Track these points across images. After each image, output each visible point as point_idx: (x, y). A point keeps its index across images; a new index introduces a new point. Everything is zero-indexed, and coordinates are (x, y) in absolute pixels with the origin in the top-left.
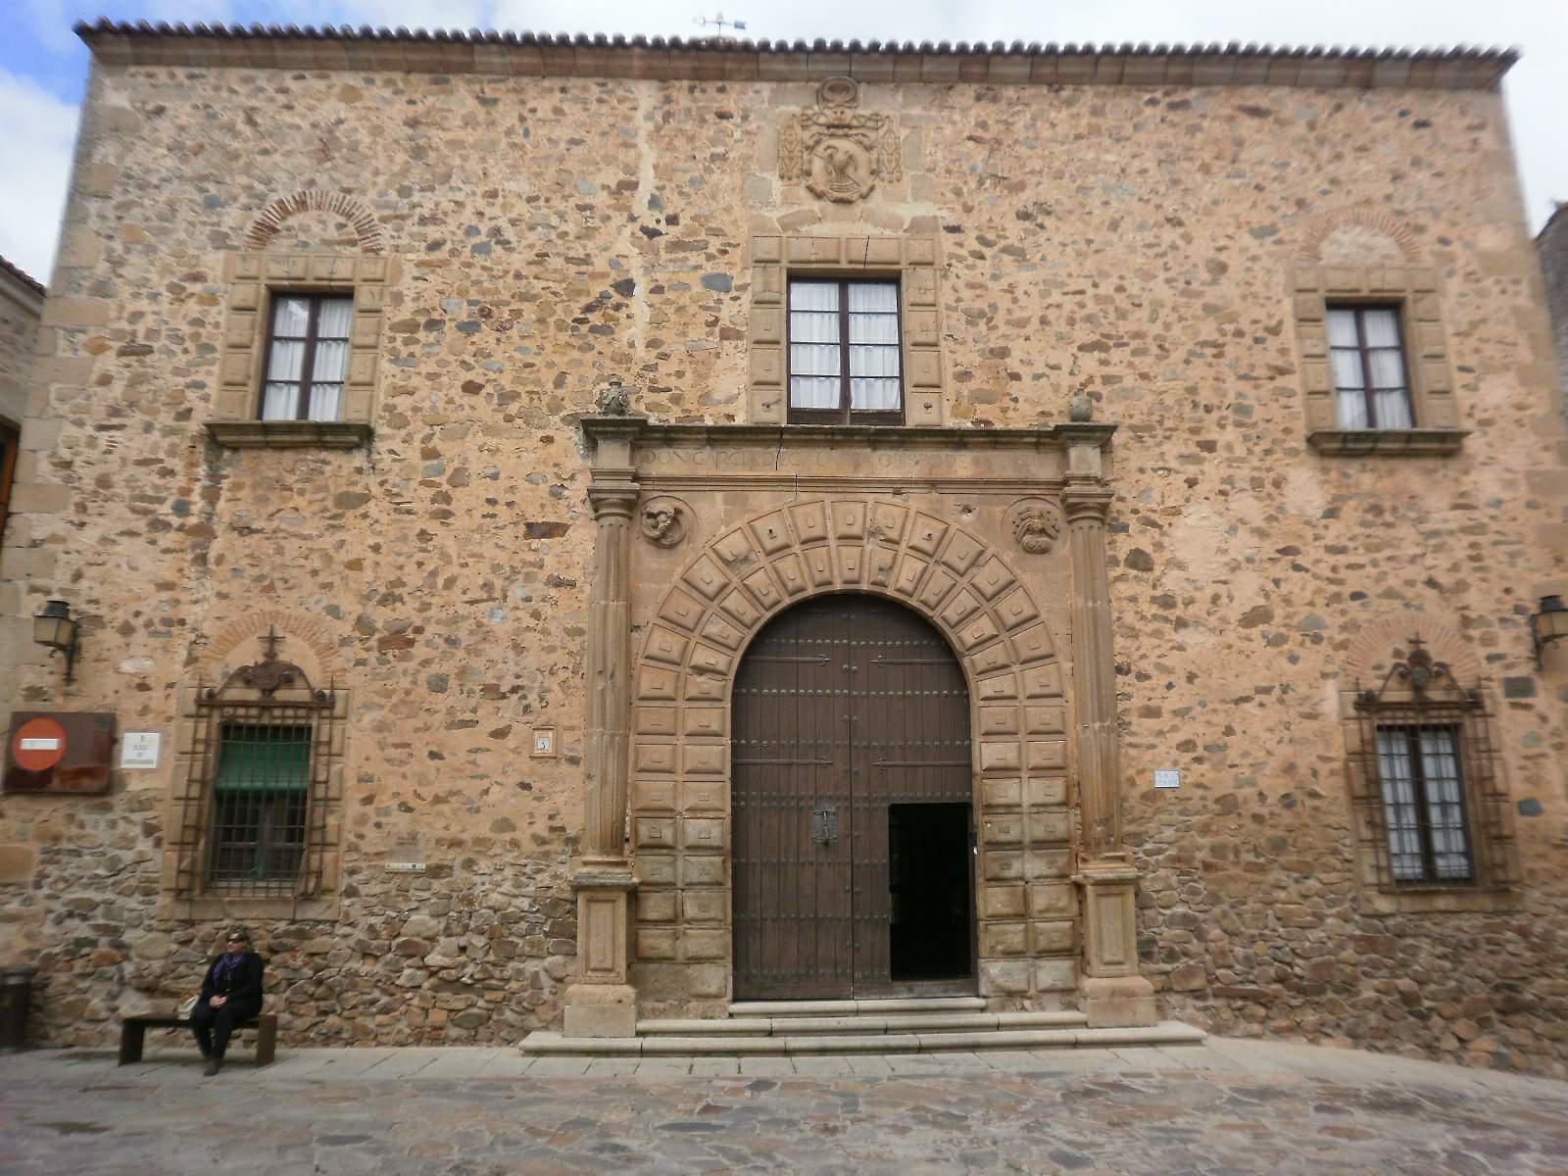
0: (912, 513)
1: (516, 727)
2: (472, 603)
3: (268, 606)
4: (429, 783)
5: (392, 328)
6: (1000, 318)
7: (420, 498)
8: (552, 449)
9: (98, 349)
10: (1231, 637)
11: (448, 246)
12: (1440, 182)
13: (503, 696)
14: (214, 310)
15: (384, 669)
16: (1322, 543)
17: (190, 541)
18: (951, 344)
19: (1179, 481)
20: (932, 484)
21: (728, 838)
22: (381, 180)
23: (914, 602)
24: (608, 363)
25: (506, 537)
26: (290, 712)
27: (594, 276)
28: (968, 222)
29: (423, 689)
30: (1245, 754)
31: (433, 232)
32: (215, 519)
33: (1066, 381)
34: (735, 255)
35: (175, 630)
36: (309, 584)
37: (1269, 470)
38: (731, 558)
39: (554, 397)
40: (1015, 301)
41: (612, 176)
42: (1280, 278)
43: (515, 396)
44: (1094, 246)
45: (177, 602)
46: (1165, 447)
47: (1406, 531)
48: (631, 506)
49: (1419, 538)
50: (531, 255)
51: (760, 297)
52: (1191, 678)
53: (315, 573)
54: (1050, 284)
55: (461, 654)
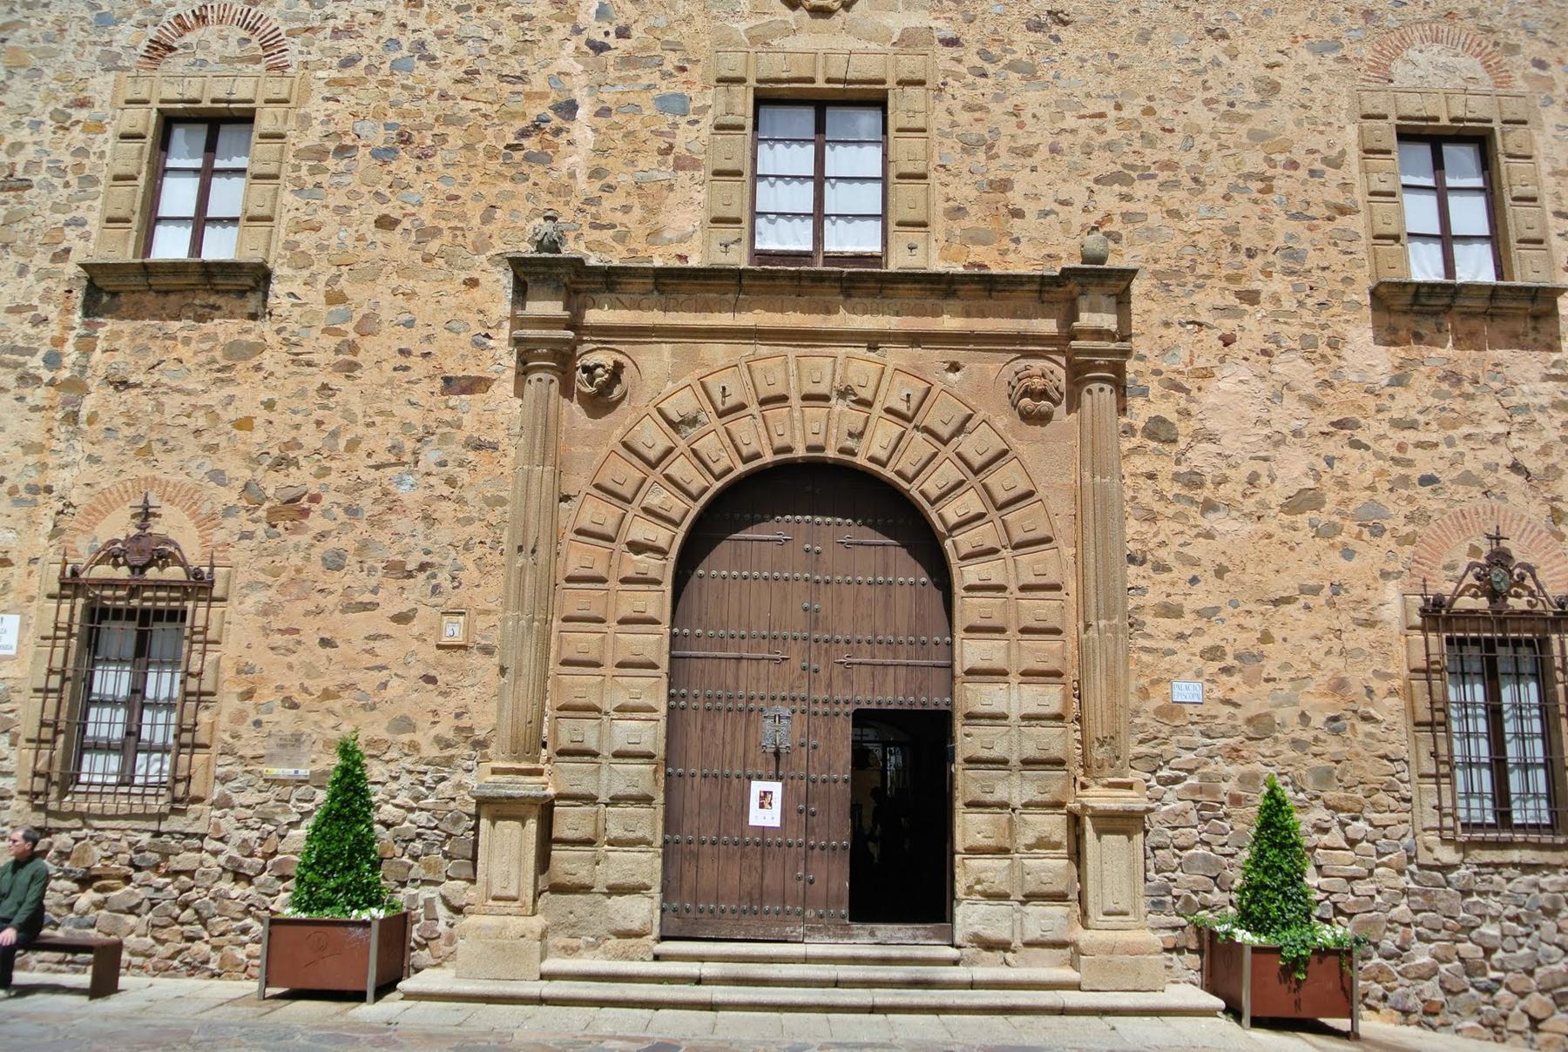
0: (889, 371)
1: (422, 611)
2: (377, 467)
3: (144, 471)
4: (321, 675)
6: (1002, 146)
7: (323, 349)
8: (476, 293)
10: (1271, 525)
11: (365, 61)
13: (410, 575)
14: (100, 138)
15: (273, 542)
16: (1386, 415)
17: (60, 397)
18: (944, 177)
19: (1212, 339)
21: (662, 745)
23: (888, 473)
24: (545, 196)
25: (420, 393)
28: (970, 35)
29: (315, 568)
30: (1286, 666)
31: (347, 46)
32: (89, 372)
33: (1078, 218)
34: (695, 72)
35: (40, 498)
36: (191, 446)
37: (1324, 327)
38: (677, 419)
39: (481, 234)
40: (1021, 125)
42: (1344, 102)
43: (436, 232)
45: (44, 466)
46: (1196, 298)
47: (1487, 404)
48: (564, 360)
49: (1504, 414)
50: (459, 72)
51: (722, 121)
53: (198, 432)
55: (362, 526)
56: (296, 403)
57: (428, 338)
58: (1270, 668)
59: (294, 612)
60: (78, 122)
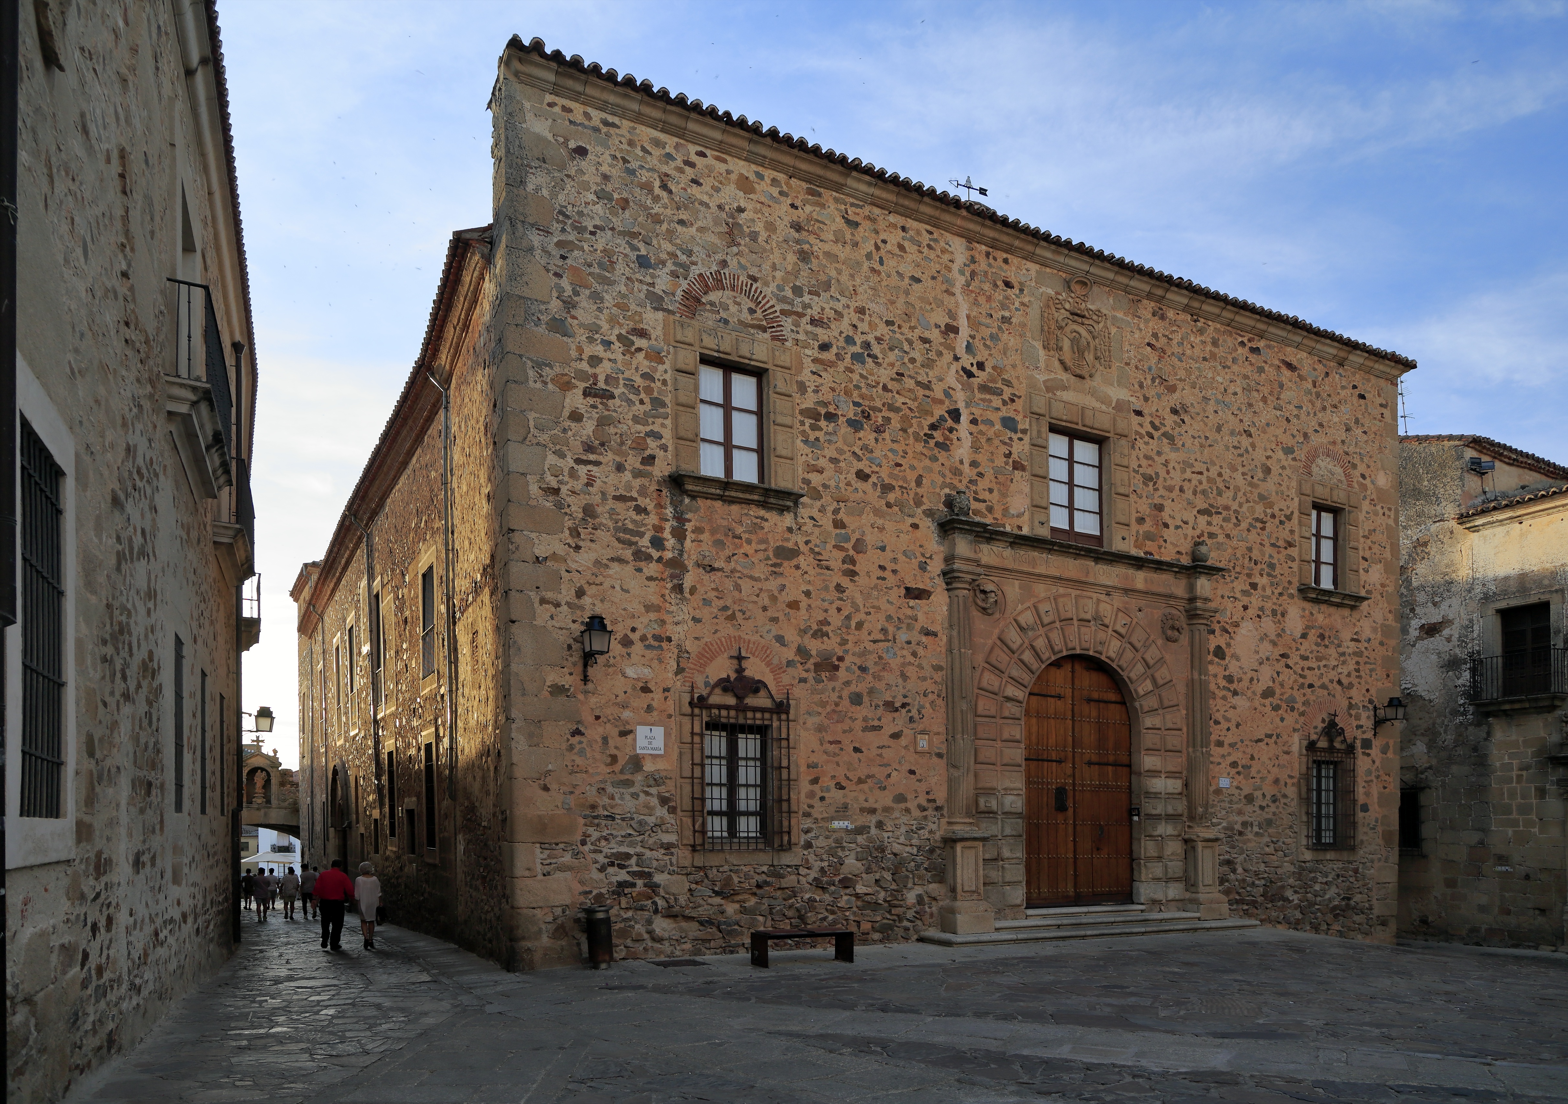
2: (875, 642)
5: (802, 412)
7: (835, 559)
8: (918, 533)
9: (566, 386)
12: (1365, 437)
14: (661, 368)
15: (821, 686)
20: (1126, 591)
26: (758, 715)
32: (685, 556)
34: (1019, 404)
35: (664, 645)
44: (1209, 442)
46: (1235, 584)
47: (1332, 651)
50: (892, 373)
53: (765, 609)
56: (824, 595)
60: (639, 350)
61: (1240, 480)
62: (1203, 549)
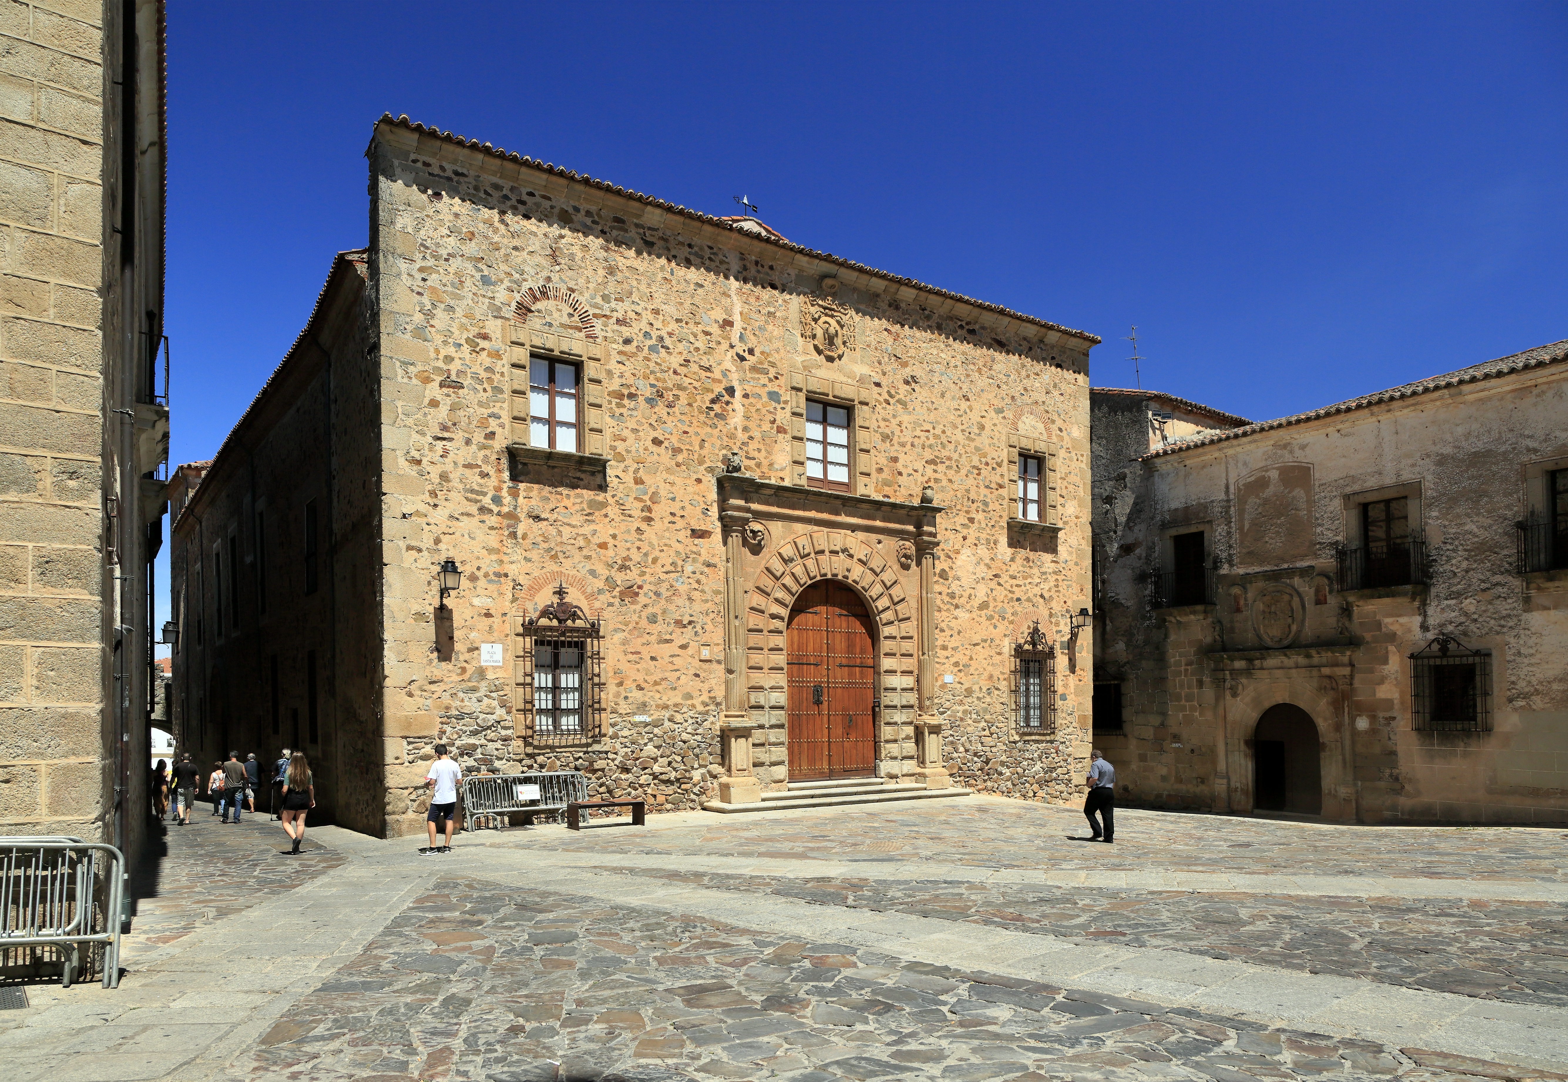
3: (555, 568)
6: (895, 441)
7: (635, 509)
8: (701, 486)
10: (974, 615)
11: (635, 344)
17: (506, 522)
19: (960, 536)
22: (591, 285)
27: (714, 380)
29: (644, 623)
34: (782, 381)
35: (503, 579)
36: (578, 556)
41: (721, 316)
43: (680, 450)
45: (502, 561)
52: (959, 633)
54: (916, 424)
56: (626, 537)
57: (683, 508)
58: (972, 670)
59: (637, 644)
61: (960, 437)
62: (929, 492)
